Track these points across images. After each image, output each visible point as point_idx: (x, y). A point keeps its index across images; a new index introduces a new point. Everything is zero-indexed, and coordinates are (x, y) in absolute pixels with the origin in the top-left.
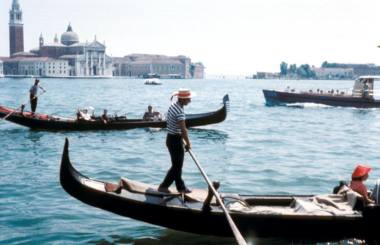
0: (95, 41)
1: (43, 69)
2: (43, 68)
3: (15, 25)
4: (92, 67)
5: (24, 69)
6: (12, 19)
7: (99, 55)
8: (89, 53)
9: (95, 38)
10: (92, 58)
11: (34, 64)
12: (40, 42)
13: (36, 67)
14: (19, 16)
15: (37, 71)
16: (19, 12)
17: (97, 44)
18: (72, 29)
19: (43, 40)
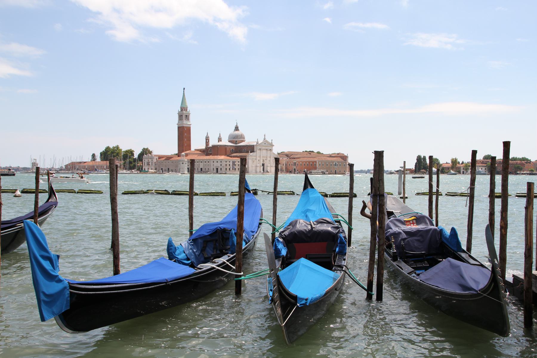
0: (264, 140)
2: (220, 166)
3: (184, 126)
4: (262, 165)
6: (181, 120)
7: (267, 153)
8: (259, 151)
9: (265, 137)
10: (261, 156)
12: (206, 141)
13: (212, 165)
14: (187, 117)
15: (213, 168)
16: (188, 113)
18: (239, 128)
19: (208, 140)
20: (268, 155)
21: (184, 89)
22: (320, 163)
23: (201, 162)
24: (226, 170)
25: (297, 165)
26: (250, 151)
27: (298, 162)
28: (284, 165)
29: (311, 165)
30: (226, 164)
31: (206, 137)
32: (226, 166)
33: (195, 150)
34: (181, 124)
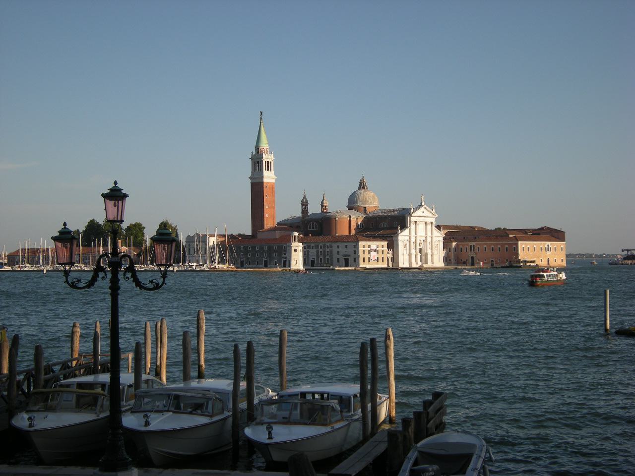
1: (353, 256)
3: (265, 180)
5: (308, 257)
7: (426, 229)
11: (331, 247)
15: (338, 259)
17: (425, 211)
20: (429, 234)
21: (262, 113)
22: (523, 246)
23: (313, 248)
24: (364, 261)
25: (476, 249)
26: (399, 227)
27: (478, 244)
28: (452, 251)
29: (507, 251)
30: (364, 251)
31: (302, 201)
32: (364, 253)
33: (278, 224)
34: (259, 178)
